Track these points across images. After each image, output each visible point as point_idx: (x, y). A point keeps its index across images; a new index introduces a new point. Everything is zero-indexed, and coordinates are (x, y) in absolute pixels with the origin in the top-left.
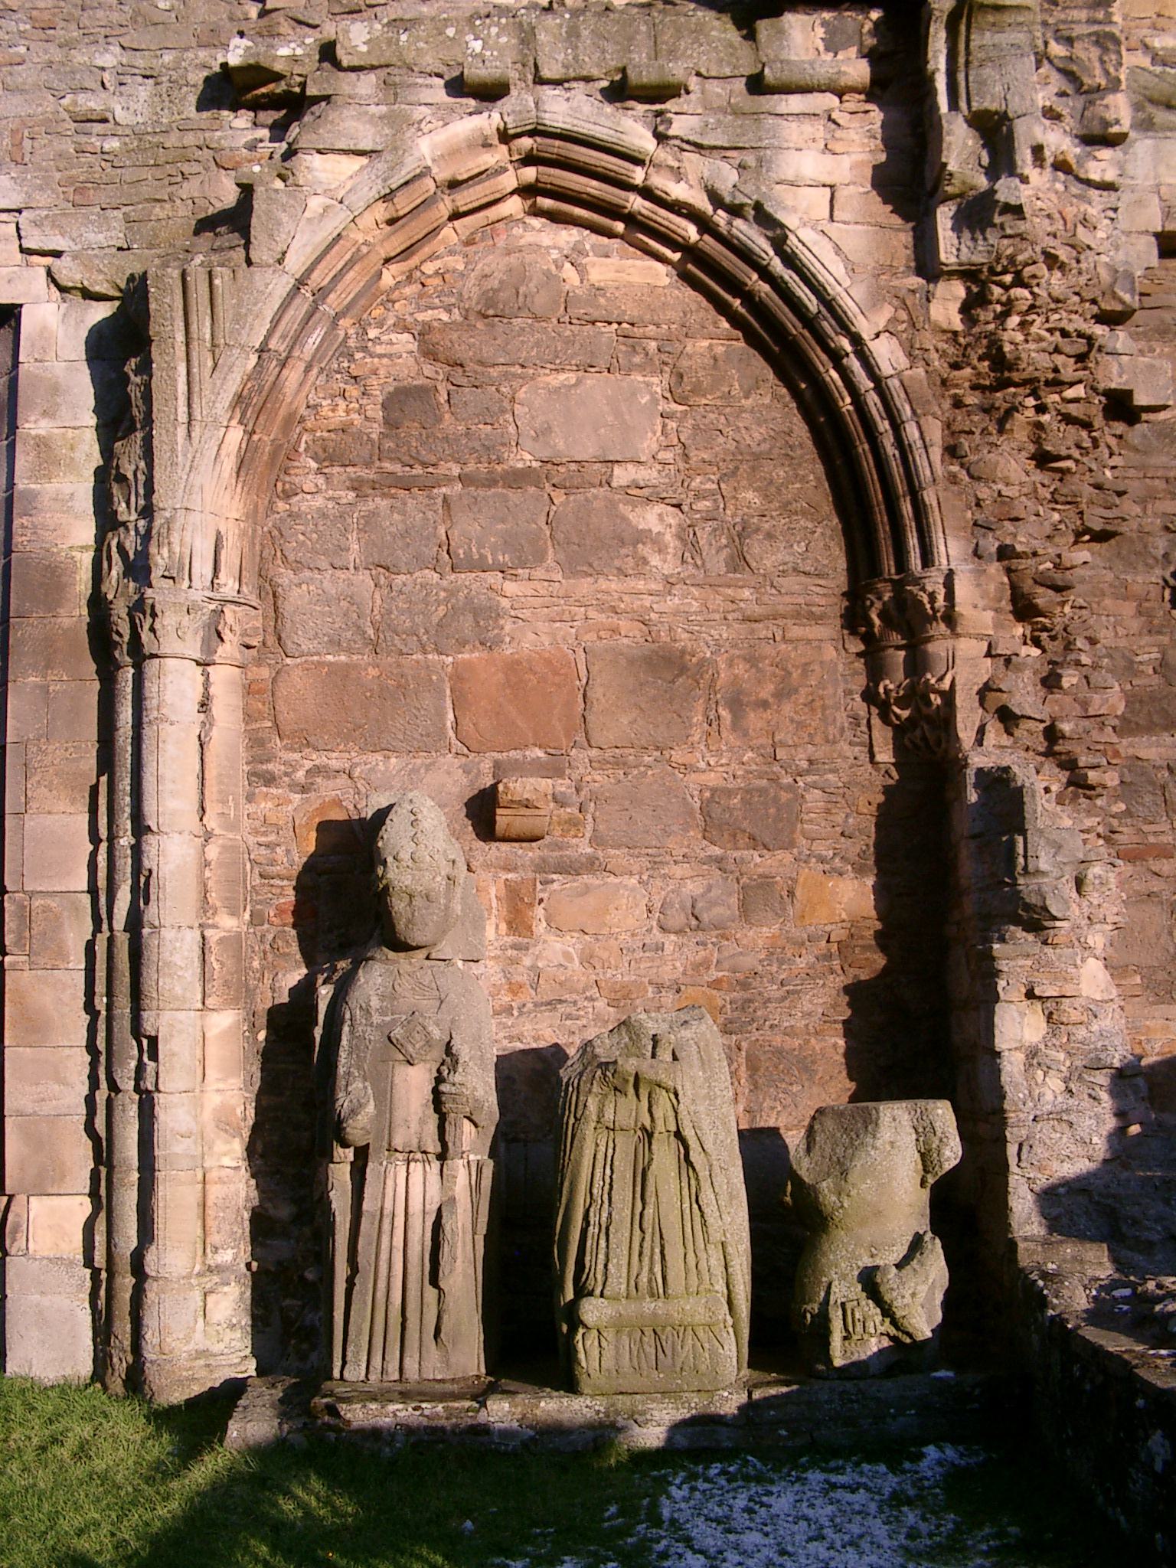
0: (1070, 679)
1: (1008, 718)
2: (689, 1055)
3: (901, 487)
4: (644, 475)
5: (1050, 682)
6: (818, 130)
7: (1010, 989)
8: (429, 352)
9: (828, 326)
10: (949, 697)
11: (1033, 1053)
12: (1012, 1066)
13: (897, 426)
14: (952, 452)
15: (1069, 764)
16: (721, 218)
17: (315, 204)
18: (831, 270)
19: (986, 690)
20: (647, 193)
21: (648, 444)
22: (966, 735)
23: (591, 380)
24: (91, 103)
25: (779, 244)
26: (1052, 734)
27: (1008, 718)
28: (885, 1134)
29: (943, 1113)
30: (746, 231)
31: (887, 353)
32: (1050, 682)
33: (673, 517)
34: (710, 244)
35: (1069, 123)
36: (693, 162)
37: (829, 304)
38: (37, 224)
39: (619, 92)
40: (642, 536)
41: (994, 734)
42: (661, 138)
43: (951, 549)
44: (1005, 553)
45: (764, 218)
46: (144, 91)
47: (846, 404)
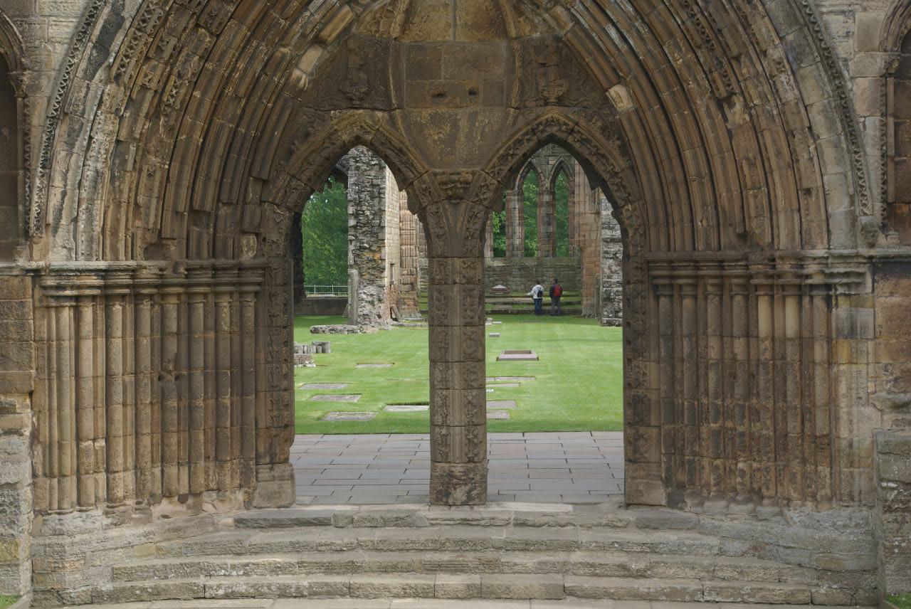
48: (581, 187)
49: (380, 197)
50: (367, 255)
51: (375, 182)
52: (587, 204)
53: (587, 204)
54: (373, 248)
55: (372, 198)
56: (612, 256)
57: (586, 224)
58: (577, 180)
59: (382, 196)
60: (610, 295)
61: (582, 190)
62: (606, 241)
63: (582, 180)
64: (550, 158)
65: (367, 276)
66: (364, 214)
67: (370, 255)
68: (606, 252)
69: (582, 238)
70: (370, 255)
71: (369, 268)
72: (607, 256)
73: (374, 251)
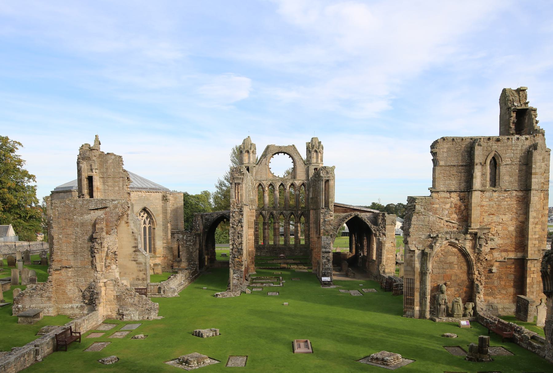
0: (482, 277)
1: (478, 280)
2: (460, 300)
3: (472, 265)
4: (455, 263)
5: (480, 278)
6: (469, 242)
7: (477, 296)
8: (442, 255)
9: (468, 255)
10: (474, 278)
11: (478, 300)
12: (477, 301)
13: (472, 262)
14: (476, 264)
15: (481, 283)
16: (462, 248)
17: (437, 247)
18: (468, 250)
19: (476, 279)
20: (457, 245)
21: (456, 261)
22: (475, 281)
23: (453, 256)
24: (420, 236)
25: (466, 250)
26: (480, 281)
27: (478, 280)
28: (470, 305)
29: (473, 303)
30: (463, 248)
31: (472, 257)
32: (480, 278)
33: (457, 266)
34: (461, 249)
35: (485, 242)
36: (460, 244)
37: (468, 253)
38: (417, 245)
39: (456, 239)
40: (455, 267)
41: (477, 281)
42: (458, 242)
43: (475, 270)
44: (478, 270)
45: (465, 248)
46: (423, 236)
47: (469, 260)
48: (313, 228)
49: (241, 238)
50: (237, 260)
51: (239, 232)
52: (315, 234)
53: (315, 234)
54: (239, 257)
55: (238, 238)
56: (325, 258)
57: (314, 241)
58: (311, 226)
59: (242, 238)
60: (325, 273)
61: (313, 230)
62: (323, 252)
63: (312, 226)
64: (299, 211)
65: (237, 268)
66: (235, 244)
67: (238, 260)
68: (324, 257)
69: (312, 246)
70: (238, 260)
71: (237, 265)
72: (324, 258)
73: (239, 258)
